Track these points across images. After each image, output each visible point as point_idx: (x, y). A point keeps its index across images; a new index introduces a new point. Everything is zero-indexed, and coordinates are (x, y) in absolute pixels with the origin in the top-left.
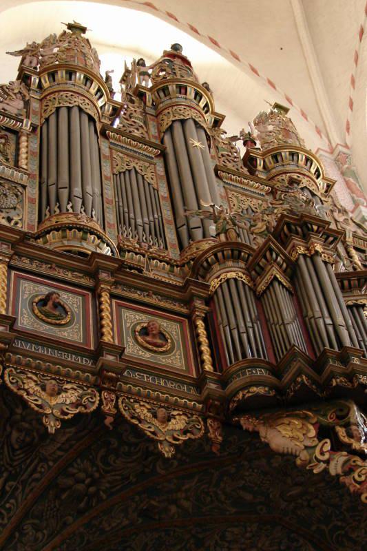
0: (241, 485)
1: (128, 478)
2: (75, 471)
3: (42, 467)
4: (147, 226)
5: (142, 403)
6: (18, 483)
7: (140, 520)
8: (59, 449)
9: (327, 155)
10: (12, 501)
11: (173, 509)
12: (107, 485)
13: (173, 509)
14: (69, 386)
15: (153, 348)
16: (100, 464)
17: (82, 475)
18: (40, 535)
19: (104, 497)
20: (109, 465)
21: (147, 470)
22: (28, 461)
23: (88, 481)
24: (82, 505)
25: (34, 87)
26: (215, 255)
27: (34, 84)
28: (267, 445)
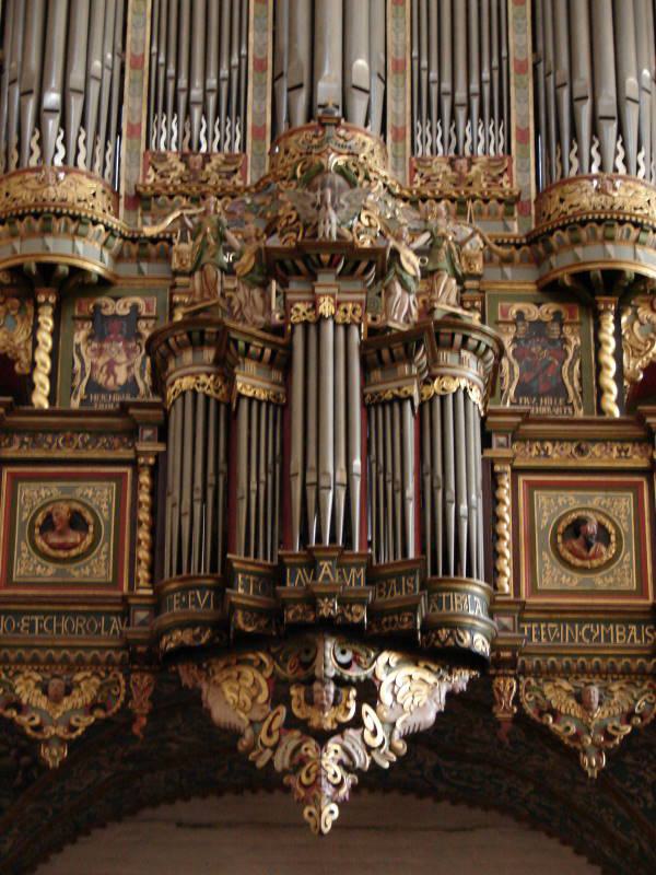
15: (62, 556)
23: (13, 753)
24: (19, 780)
28: (209, 712)
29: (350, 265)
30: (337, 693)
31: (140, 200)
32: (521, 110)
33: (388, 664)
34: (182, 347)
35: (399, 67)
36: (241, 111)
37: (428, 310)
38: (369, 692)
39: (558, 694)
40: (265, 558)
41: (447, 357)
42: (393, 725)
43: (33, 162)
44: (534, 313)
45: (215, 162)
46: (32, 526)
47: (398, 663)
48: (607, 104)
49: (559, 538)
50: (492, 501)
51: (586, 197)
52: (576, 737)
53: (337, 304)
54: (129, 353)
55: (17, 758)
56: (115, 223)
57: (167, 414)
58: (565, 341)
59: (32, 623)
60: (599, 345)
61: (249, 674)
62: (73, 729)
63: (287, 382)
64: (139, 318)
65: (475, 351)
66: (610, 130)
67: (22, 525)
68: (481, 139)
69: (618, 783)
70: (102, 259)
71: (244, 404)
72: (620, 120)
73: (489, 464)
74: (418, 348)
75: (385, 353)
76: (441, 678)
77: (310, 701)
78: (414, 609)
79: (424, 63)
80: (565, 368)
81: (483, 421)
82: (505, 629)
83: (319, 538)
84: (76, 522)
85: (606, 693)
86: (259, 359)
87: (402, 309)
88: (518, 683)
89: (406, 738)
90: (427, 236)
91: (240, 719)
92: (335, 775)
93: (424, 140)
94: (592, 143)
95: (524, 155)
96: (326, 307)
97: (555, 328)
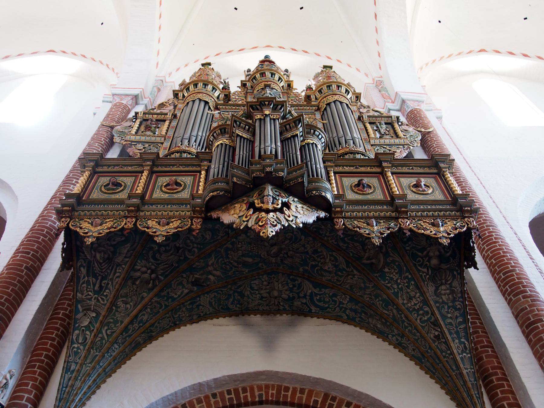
0: (241, 254)
1: (173, 265)
2: (139, 267)
3: (119, 269)
4: (199, 138)
5: (152, 219)
6: (108, 281)
7: (195, 288)
8: (125, 257)
9: (371, 85)
10: (107, 291)
11: (210, 277)
12: (162, 271)
13: (210, 277)
16: (152, 261)
17: (144, 269)
18: (128, 306)
19: (162, 278)
20: (158, 260)
21: (181, 258)
22: (110, 268)
23: (149, 271)
24: (150, 285)
25: (181, 98)
26: (213, 135)
27: (180, 97)
29: (275, 106)
55: (151, 274)
69: (383, 282)
74: (299, 124)
75: (288, 127)
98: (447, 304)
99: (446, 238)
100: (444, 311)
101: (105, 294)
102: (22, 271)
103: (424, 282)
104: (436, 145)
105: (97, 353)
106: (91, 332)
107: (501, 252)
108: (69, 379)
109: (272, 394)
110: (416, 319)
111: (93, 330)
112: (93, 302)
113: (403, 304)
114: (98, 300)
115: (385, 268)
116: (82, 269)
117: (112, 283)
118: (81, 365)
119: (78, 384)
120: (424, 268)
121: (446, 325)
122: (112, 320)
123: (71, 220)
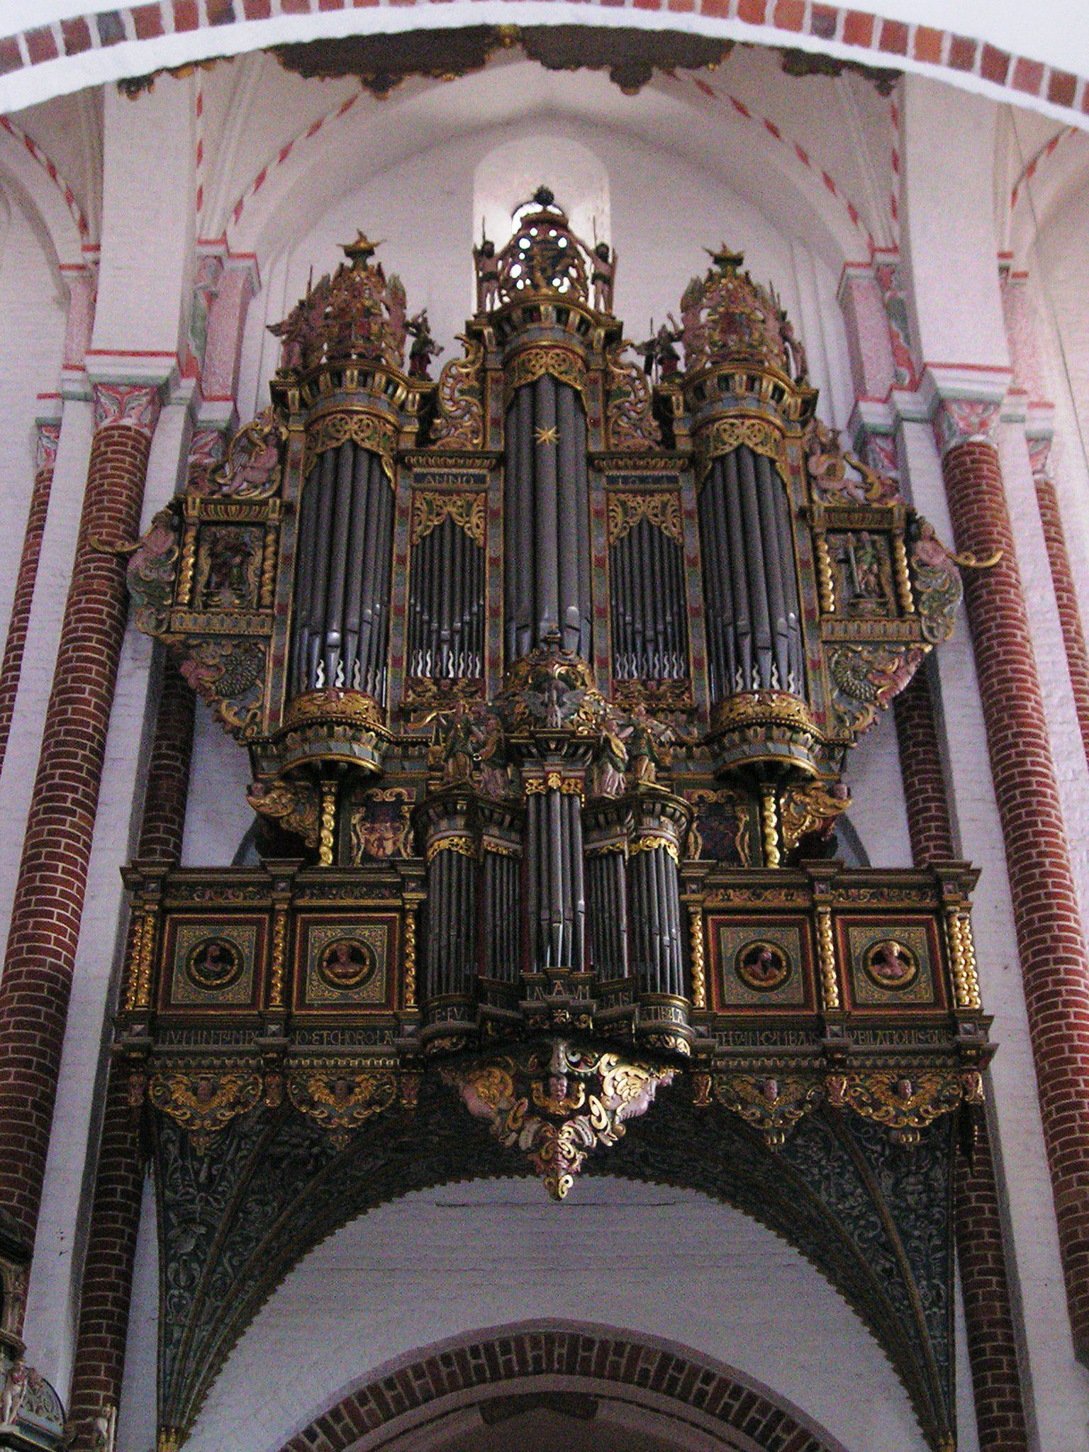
8: (258, 1123)
14: (224, 1081)
17: (295, 1141)
18: (268, 1209)
23: (307, 1143)
28: (465, 1106)
30: (569, 1087)
31: (402, 714)
32: (698, 644)
33: (609, 1063)
34: (440, 817)
35: (602, 613)
36: (480, 648)
37: (633, 785)
38: (595, 1084)
39: (745, 1086)
40: (509, 979)
41: (649, 821)
42: (614, 1112)
43: (319, 685)
44: (712, 796)
45: (461, 685)
46: (321, 960)
47: (617, 1062)
48: (764, 635)
49: (742, 965)
50: (688, 936)
51: (749, 707)
52: (761, 1121)
53: (563, 779)
54: (396, 830)
55: (310, 1148)
56: (384, 730)
57: (428, 870)
58: (738, 819)
59: (321, 1036)
60: (764, 820)
61: (497, 1072)
62: (355, 1120)
63: (524, 841)
64: (404, 803)
65: (671, 817)
66: (766, 658)
67: (313, 958)
68: (668, 668)
70: (373, 759)
71: (490, 861)
72: (773, 647)
73: (684, 906)
75: (601, 818)
76: (651, 1075)
77: (547, 1093)
78: (629, 1017)
79: (621, 610)
80: (738, 838)
81: (679, 871)
82: (701, 1035)
83: (553, 962)
84: (356, 956)
85: (782, 1085)
86: (500, 824)
87: (614, 782)
88: (713, 1079)
89: (625, 1122)
90: (631, 729)
91: (488, 1110)
92: (569, 1152)
93: (622, 666)
94: (753, 667)
95: (700, 678)
96: (554, 781)
97: (728, 808)
98: (915, 1211)
99: (914, 1130)
100: (906, 1227)
101: (220, 1189)
102: (27, 1116)
103: (873, 1169)
104: (999, 626)
105: (219, 1303)
106: (201, 1263)
107: (1066, 1046)
108: (174, 1359)
109: (560, 1355)
110: (852, 1234)
111: (205, 1260)
112: (198, 1207)
113: (829, 1203)
114: (208, 1203)
115: (795, 1138)
116: (170, 1146)
117: (233, 1170)
118: (191, 1330)
119: (191, 1365)
120: (876, 1144)
121: (907, 1252)
122: (238, 1239)
123: (149, 1079)
